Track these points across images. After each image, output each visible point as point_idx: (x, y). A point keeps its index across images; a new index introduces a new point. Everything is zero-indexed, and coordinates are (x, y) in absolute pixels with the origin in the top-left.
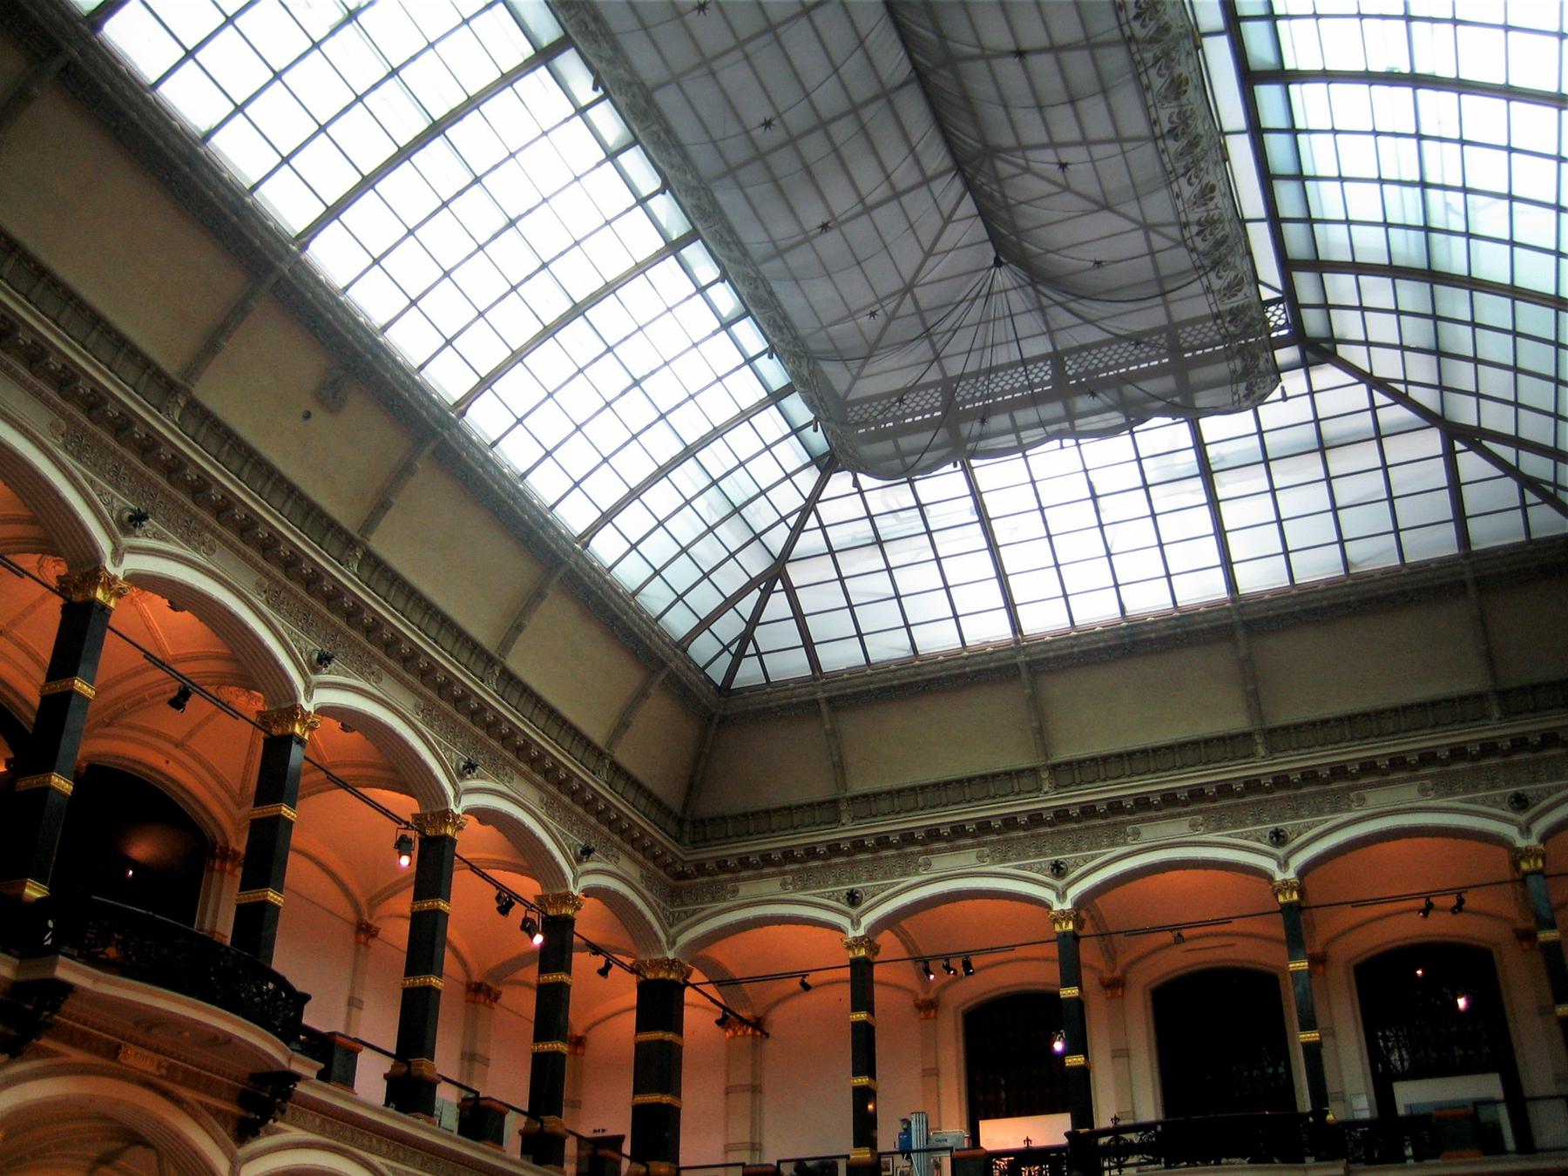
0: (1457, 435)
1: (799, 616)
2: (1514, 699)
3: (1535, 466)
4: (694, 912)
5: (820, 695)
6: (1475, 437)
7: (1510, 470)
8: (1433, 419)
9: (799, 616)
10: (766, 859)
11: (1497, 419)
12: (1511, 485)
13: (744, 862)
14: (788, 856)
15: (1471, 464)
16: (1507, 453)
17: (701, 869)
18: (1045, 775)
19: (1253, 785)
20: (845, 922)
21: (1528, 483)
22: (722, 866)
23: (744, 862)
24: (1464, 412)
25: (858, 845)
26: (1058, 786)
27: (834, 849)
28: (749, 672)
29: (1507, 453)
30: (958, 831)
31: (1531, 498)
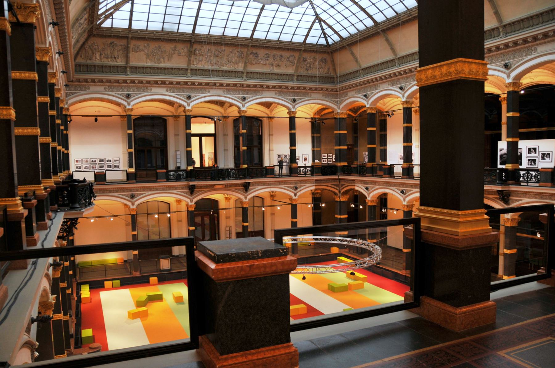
0: (318, 18)
1: (132, 11)
2: (300, 78)
3: (329, 31)
4: (75, 93)
5: (130, 36)
6: (320, 20)
7: (322, 29)
8: (317, 15)
9: (132, 11)
10: (101, 81)
11: (331, 22)
12: (321, 31)
13: (93, 81)
14: (109, 81)
15: (317, 25)
16: (325, 26)
17: (79, 80)
18: (189, 71)
19: (242, 85)
20: (125, 103)
21: (325, 34)
22: (86, 81)
23: (93, 81)
24: (323, 16)
25: (133, 82)
26: (192, 74)
27: (125, 82)
28: (107, 24)
29: (325, 26)
30: (164, 83)
31: (322, 36)
